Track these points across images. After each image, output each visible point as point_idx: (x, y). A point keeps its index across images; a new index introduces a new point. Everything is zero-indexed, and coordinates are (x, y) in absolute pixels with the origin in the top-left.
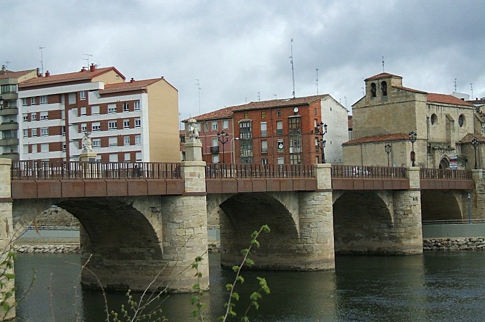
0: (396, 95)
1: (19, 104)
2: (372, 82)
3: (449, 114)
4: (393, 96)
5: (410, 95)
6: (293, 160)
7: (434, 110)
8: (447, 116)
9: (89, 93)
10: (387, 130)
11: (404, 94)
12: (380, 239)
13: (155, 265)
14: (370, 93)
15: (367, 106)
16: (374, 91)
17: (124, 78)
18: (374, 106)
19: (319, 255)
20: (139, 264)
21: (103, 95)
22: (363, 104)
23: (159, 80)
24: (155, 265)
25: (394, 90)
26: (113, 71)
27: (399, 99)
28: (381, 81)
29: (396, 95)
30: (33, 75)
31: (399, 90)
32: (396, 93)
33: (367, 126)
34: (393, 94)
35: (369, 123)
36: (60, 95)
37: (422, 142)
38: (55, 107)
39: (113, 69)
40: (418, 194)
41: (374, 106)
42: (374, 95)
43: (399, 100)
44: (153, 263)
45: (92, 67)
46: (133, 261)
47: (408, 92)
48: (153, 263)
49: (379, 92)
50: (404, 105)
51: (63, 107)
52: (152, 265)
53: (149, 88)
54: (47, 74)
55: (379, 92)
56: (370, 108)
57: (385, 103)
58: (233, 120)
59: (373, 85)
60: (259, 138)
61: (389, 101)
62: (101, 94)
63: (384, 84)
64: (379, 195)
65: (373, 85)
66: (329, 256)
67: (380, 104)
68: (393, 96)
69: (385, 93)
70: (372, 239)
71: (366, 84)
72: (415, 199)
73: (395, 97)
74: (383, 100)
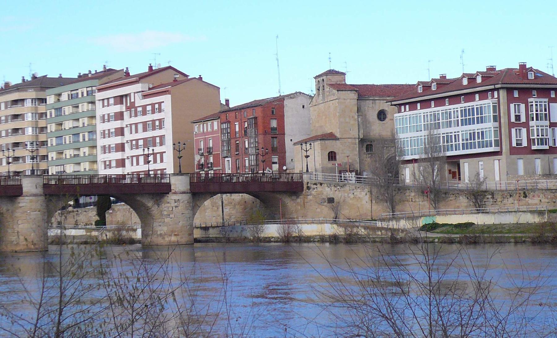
1: (99, 104)
6: (251, 160)
9: (136, 94)
17: (187, 76)
21: (145, 96)
26: (170, 70)
36: (122, 97)
37: (350, 140)
38: (118, 108)
39: (170, 67)
51: (124, 109)
58: (219, 120)
60: (234, 138)
62: (144, 96)
63: (323, 80)
64: (139, 198)
67: (322, 102)
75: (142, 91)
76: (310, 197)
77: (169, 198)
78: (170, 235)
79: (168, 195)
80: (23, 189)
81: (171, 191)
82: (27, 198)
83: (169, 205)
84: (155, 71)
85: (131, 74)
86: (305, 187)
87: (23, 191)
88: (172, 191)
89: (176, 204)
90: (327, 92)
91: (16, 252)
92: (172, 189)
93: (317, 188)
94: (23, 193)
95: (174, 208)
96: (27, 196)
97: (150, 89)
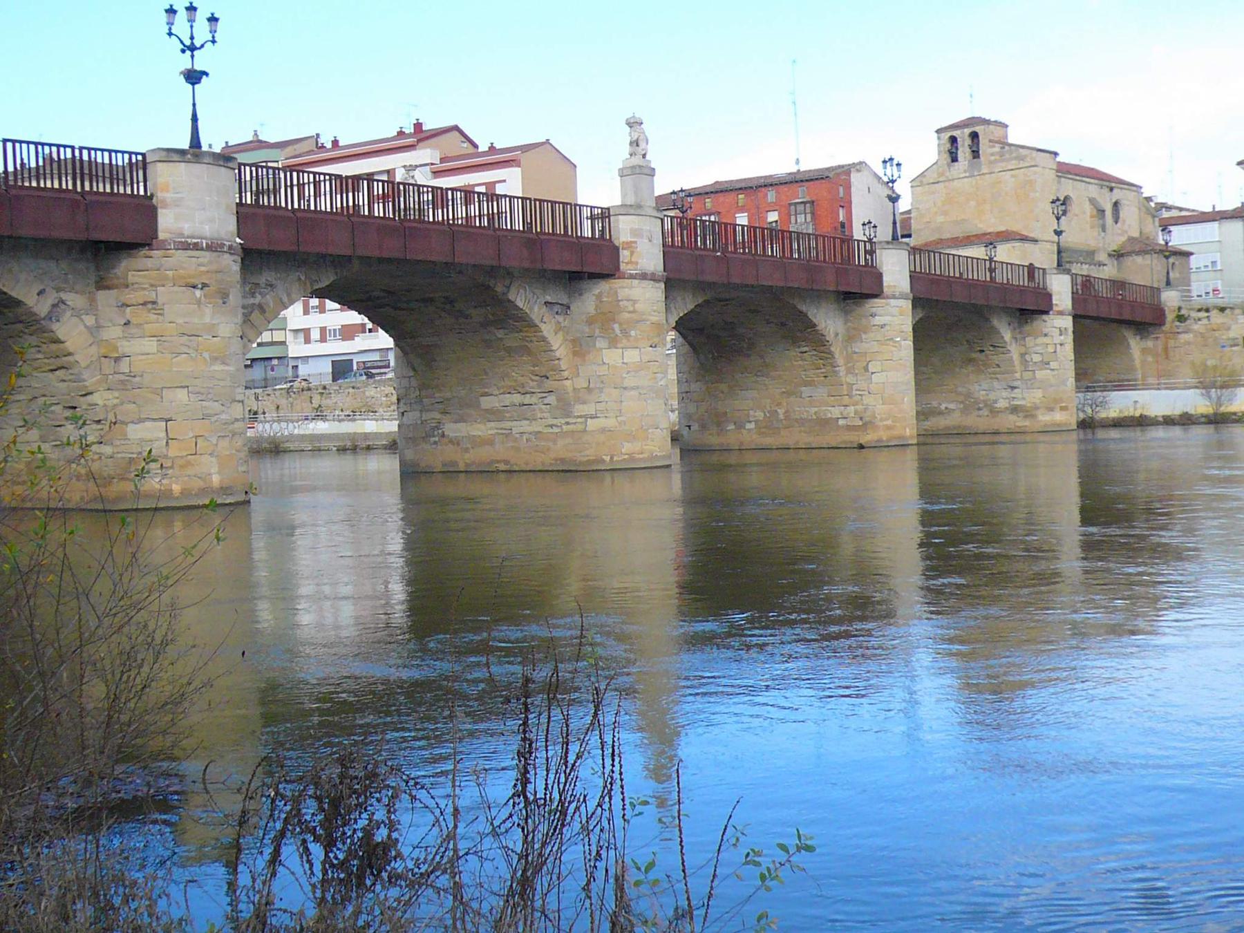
0: (998, 157)
2: (949, 134)
3: (1094, 199)
4: (993, 158)
5: (1026, 156)
7: (1069, 188)
8: (1092, 201)
10: (980, 226)
11: (1014, 155)
12: (991, 411)
13: (556, 430)
14: (947, 157)
15: (941, 179)
16: (954, 150)
17: (476, 146)
18: (953, 180)
19: (889, 428)
20: (522, 430)
21: (437, 173)
22: (932, 177)
23: (543, 144)
24: (556, 430)
25: (994, 147)
26: (457, 134)
27: (1004, 164)
28: (967, 131)
29: (998, 157)
30: (310, 145)
31: (1003, 148)
32: (997, 153)
33: (940, 219)
34: (992, 154)
35: (945, 213)
36: (357, 179)
37: (1048, 246)
39: (456, 128)
40: (1067, 322)
41: (953, 180)
42: (954, 159)
43: (1003, 165)
44: (551, 426)
45: (418, 126)
46: (508, 424)
47: (1021, 150)
48: (551, 426)
49: (964, 152)
50: (1013, 176)
52: (551, 430)
53: (525, 158)
54: (335, 143)
55: (964, 152)
56: (947, 184)
57: (976, 173)
59: (953, 140)
61: (984, 171)
63: (974, 136)
65: (953, 140)
66: (908, 430)
67: (967, 174)
68: (993, 158)
69: (976, 154)
70: (976, 413)
71: (939, 138)
72: (1062, 332)
73: (996, 161)
74: (971, 165)
75: (432, 164)
76: (1184, 337)
77: (1048, 324)
78: (1051, 409)
79: (1045, 317)
80: (885, 279)
81: (1052, 309)
82: (893, 302)
83: (1045, 340)
84: (428, 134)
85: (341, 144)
86: (1170, 317)
87: (885, 284)
88: (1055, 308)
89: (1062, 337)
90: (992, 154)
91: (861, 447)
92: (1054, 302)
93: (1208, 317)
94: (885, 290)
95: (1058, 346)
96: (894, 297)
97: (442, 160)
